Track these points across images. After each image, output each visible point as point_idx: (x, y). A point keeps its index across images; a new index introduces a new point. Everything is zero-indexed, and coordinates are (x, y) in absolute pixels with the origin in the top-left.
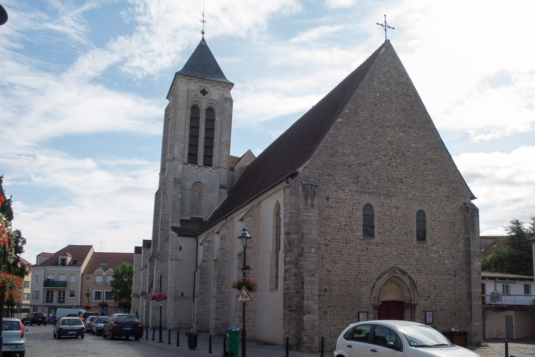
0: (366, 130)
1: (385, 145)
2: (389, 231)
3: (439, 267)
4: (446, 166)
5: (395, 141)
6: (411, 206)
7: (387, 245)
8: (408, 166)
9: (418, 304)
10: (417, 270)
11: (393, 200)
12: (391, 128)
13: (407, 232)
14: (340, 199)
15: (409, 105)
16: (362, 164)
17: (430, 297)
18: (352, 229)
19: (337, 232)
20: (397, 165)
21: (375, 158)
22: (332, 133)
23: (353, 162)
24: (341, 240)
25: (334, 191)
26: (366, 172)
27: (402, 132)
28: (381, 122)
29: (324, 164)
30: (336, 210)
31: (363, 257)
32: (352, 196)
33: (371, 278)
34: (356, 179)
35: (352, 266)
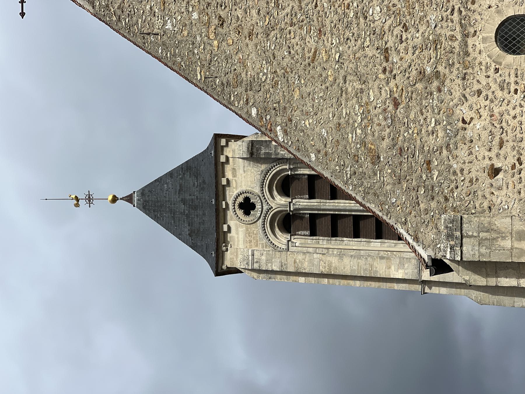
0: (292, 52)
14: (491, 133)
16: (385, 64)
21: (362, 20)
22: (317, 158)
23: (383, 92)
25: (471, 153)
26: (406, 49)
29: (399, 183)
32: (479, 92)
34: (429, 81)
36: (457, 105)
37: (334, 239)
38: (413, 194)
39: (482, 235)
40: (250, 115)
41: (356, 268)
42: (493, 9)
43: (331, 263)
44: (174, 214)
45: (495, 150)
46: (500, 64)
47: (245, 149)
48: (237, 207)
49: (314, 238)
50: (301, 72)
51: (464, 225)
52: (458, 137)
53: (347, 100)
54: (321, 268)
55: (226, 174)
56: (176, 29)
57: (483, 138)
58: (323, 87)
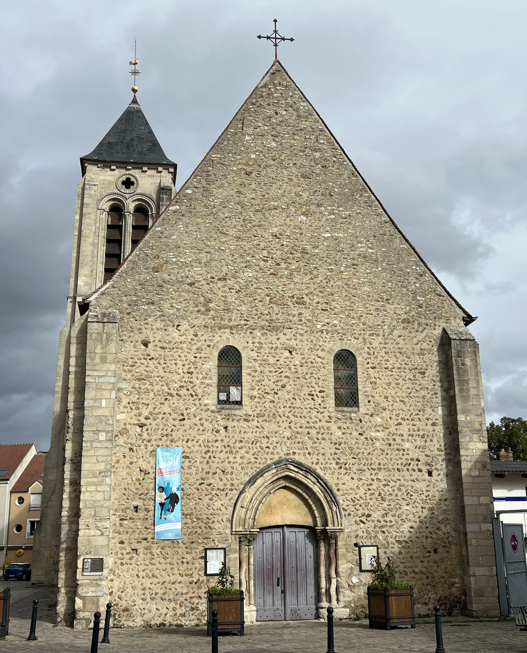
0: (227, 219)
1: (267, 240)
2: (273, 392)
3: (388, 457)
4: (402, 265)
5: (288, 231)
6: (321, 344)
7: (268, 419)
8: (315, 272)
9: (342, 530)
10: (337, 463)
11: (281, 335)
12: (280, 210)
13: (313, 393)
15: (319, 166)
16: (216, 278)
17: (369, 516)
18: (194, 394)
19: (163, 401)
20: (291, 274)
21: (244, 265)
22: (158, 232)
23: (199, 276)
24: (170, 414)
25: (158, 329)
27: (303, 214)
28: (258, 202)
29: (140, 284)
30: (162, 362)
31: (217, 444)
32: (196, 335)
33: (233, 482)
34: (205, 305)
35: (193, 461)
36: (188, 322)
37: (105, 240)
38: (133, 293)
39: (105, 335)
40: (187, 189)
41: (85, 254)
42: (246, 345)
43: (89, 238)
44: (124, 132)
45: (160, 344)
46: (213, 348)
47: (166, 185)
48: (128, 176)
49: (106, 227)
50: (214, 224)
51: (111, 324)
52: (168, 322)
53: (195, 253)
54: (85, 231)
55: (150, 171)
56: (245, 142)
57: (168, 337)
58: (204, 238)
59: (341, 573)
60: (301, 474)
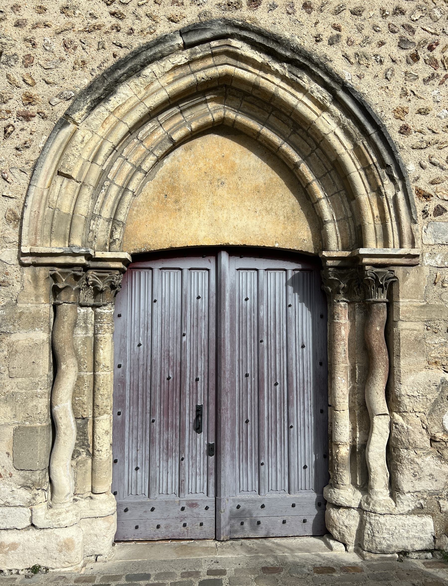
33: (33, 92)
59: (406, 401)
60: (276, 73)
